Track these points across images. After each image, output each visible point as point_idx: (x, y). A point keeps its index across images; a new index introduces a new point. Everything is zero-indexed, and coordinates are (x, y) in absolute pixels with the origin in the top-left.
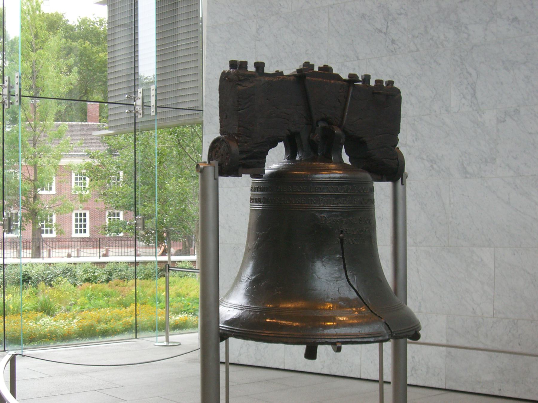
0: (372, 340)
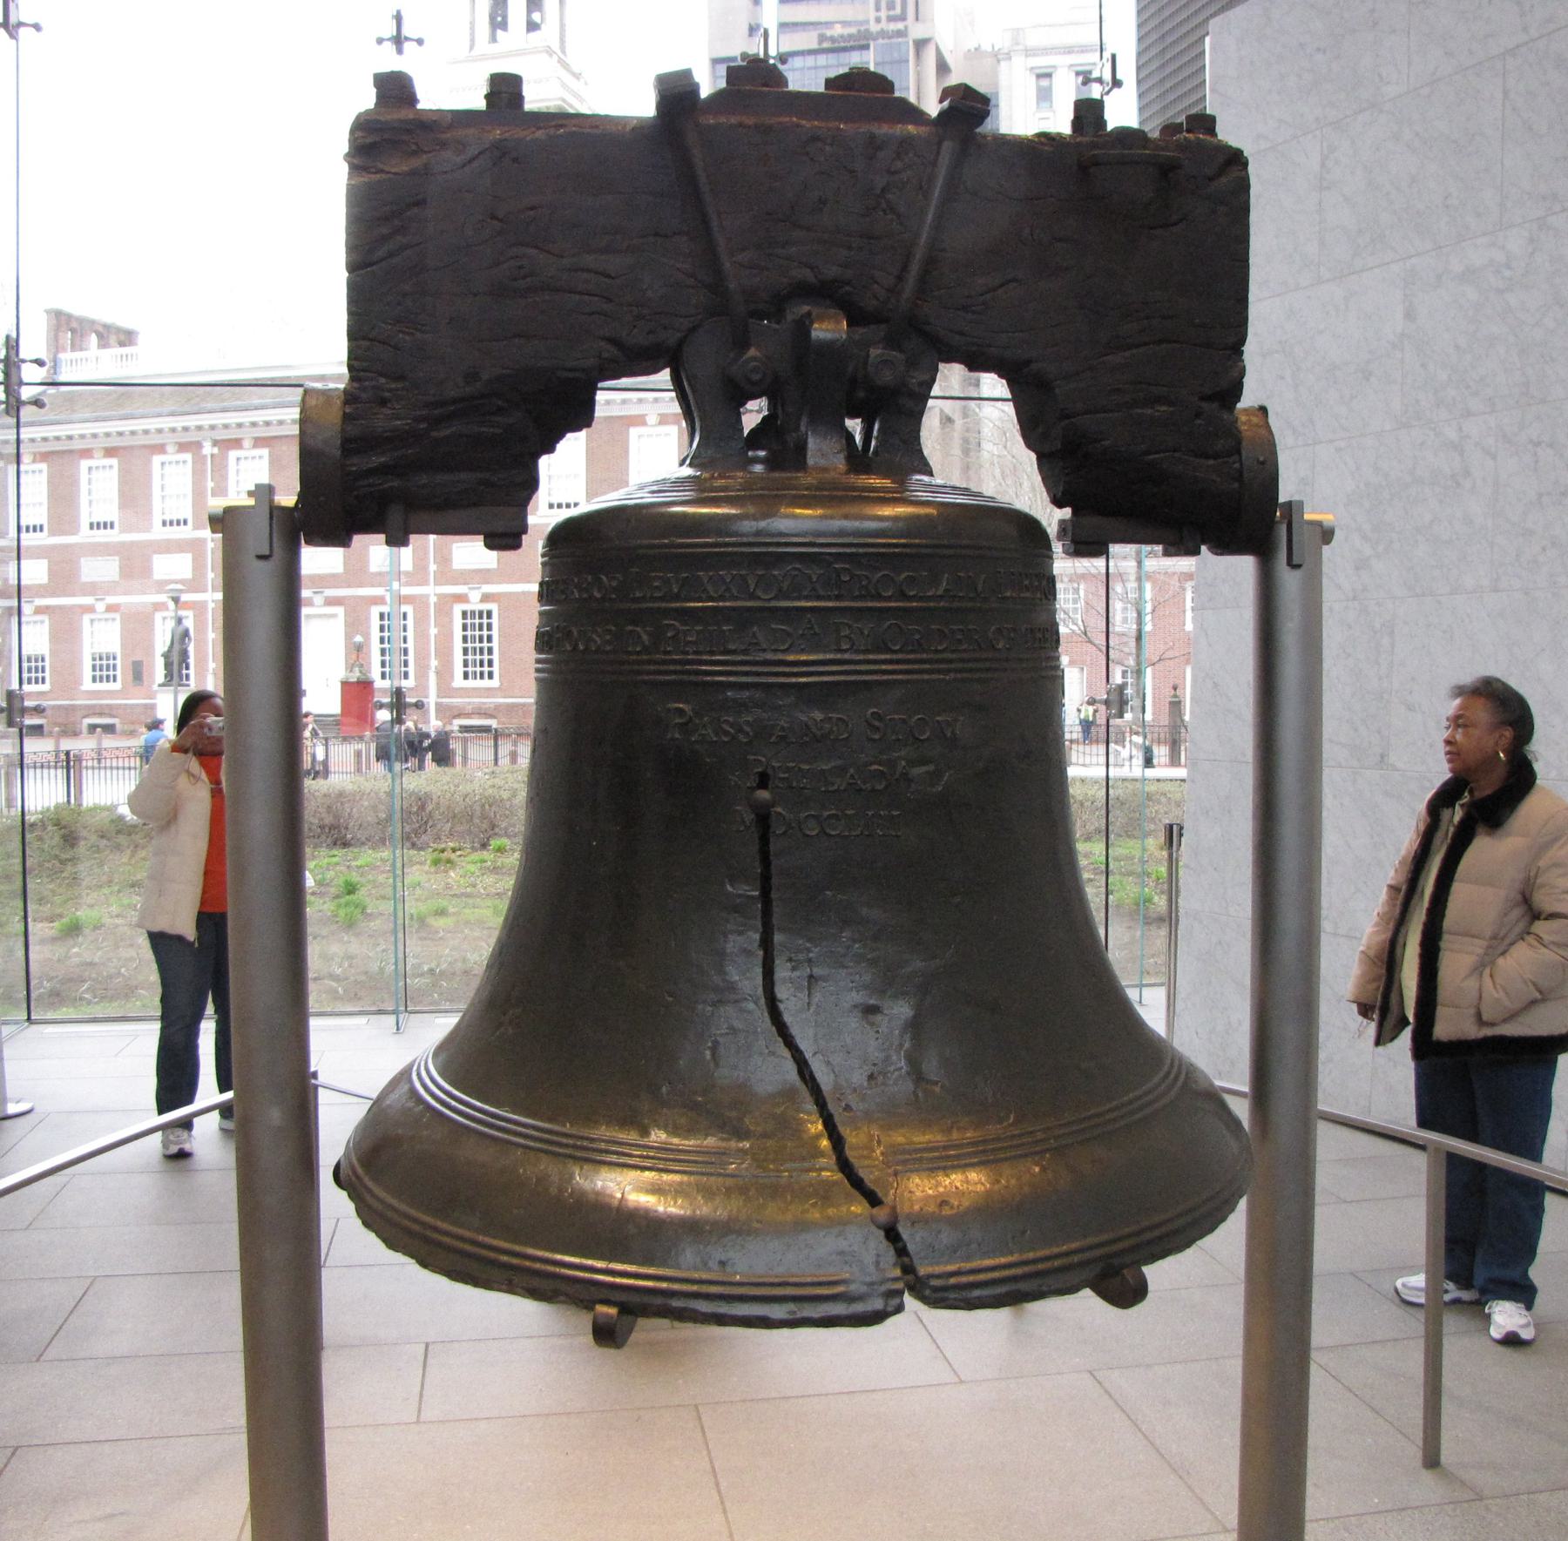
0: (777, 1312)
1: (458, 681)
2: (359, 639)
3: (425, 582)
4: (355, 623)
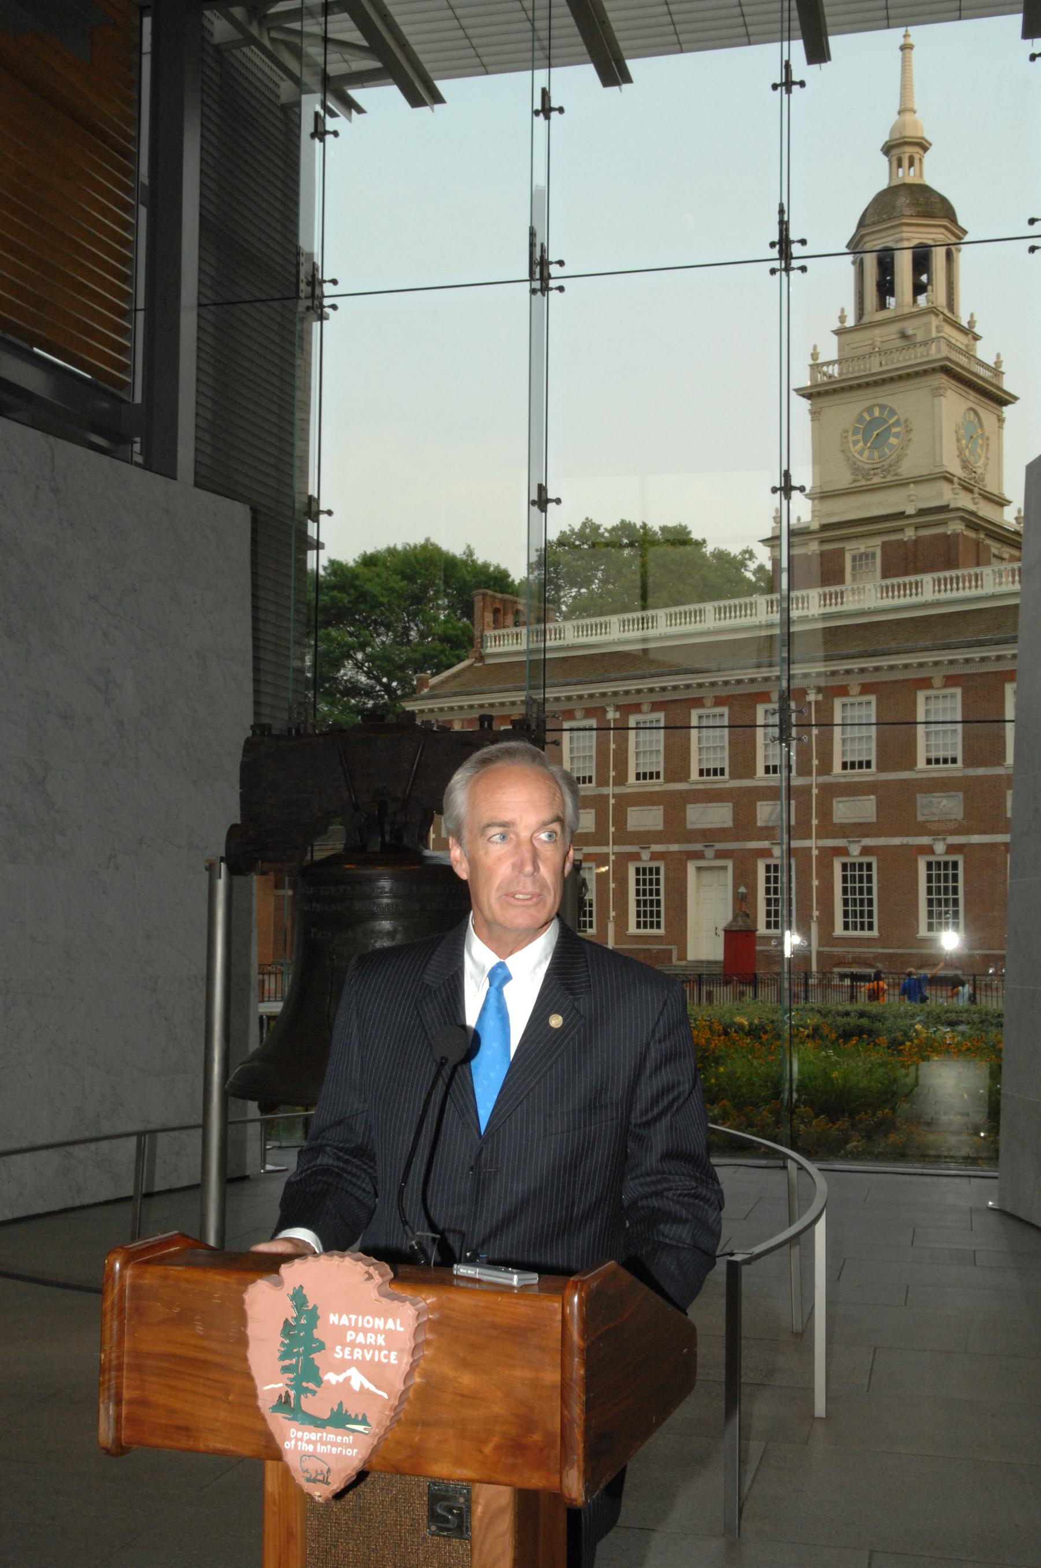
1: (839, 931)
2: (742, 890)
3: (809, 837)
4: (744, 876)
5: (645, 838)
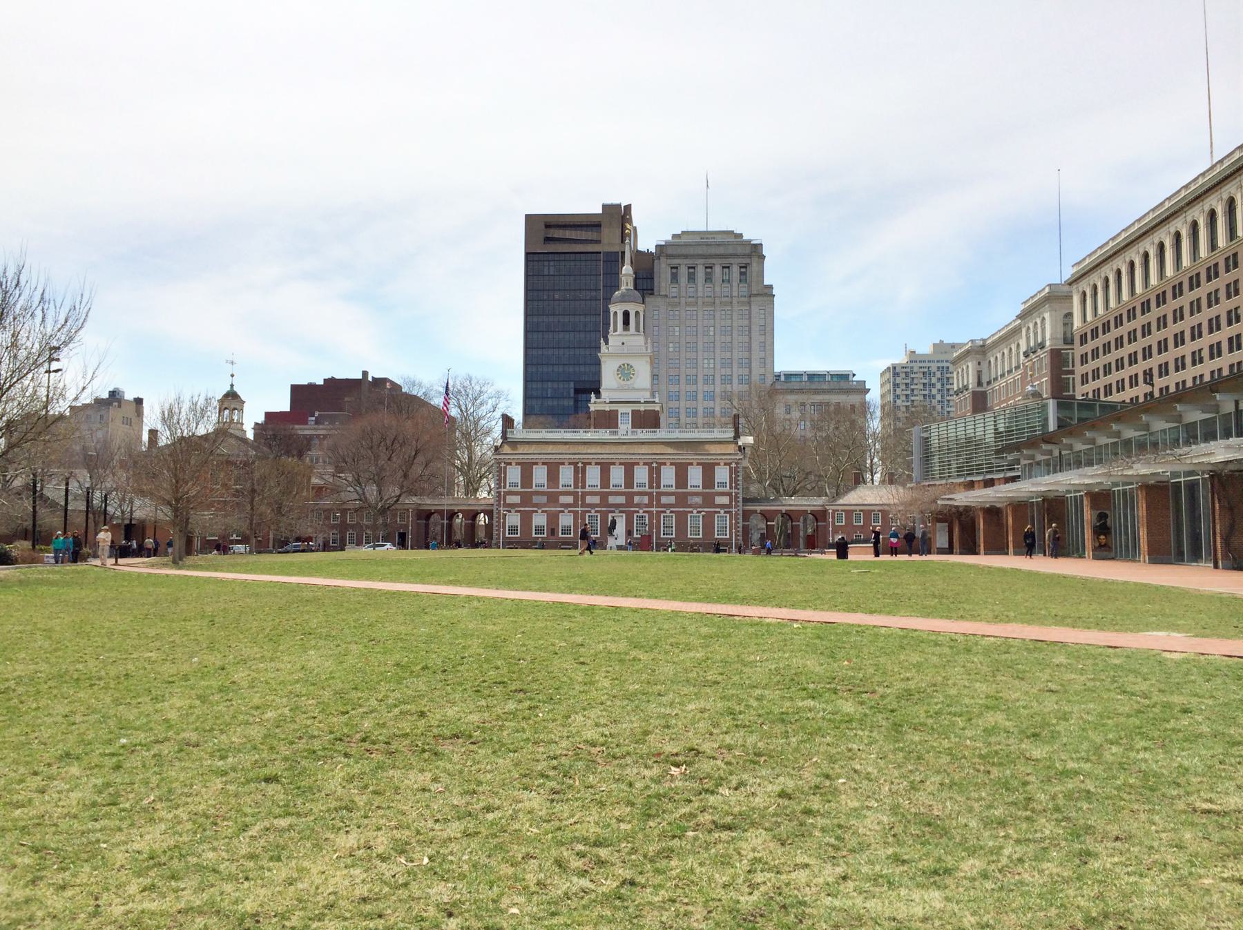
5: (592, 506)
